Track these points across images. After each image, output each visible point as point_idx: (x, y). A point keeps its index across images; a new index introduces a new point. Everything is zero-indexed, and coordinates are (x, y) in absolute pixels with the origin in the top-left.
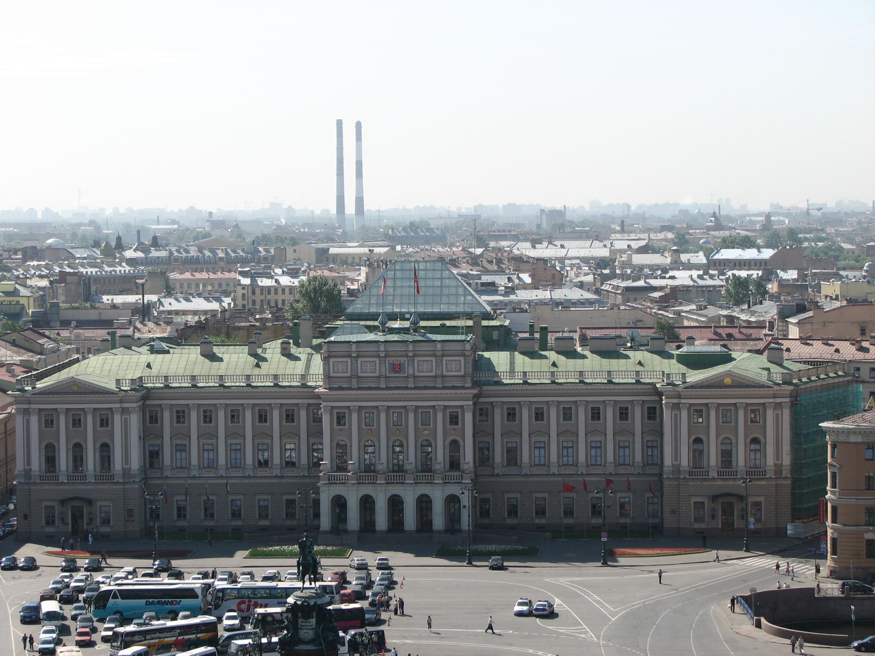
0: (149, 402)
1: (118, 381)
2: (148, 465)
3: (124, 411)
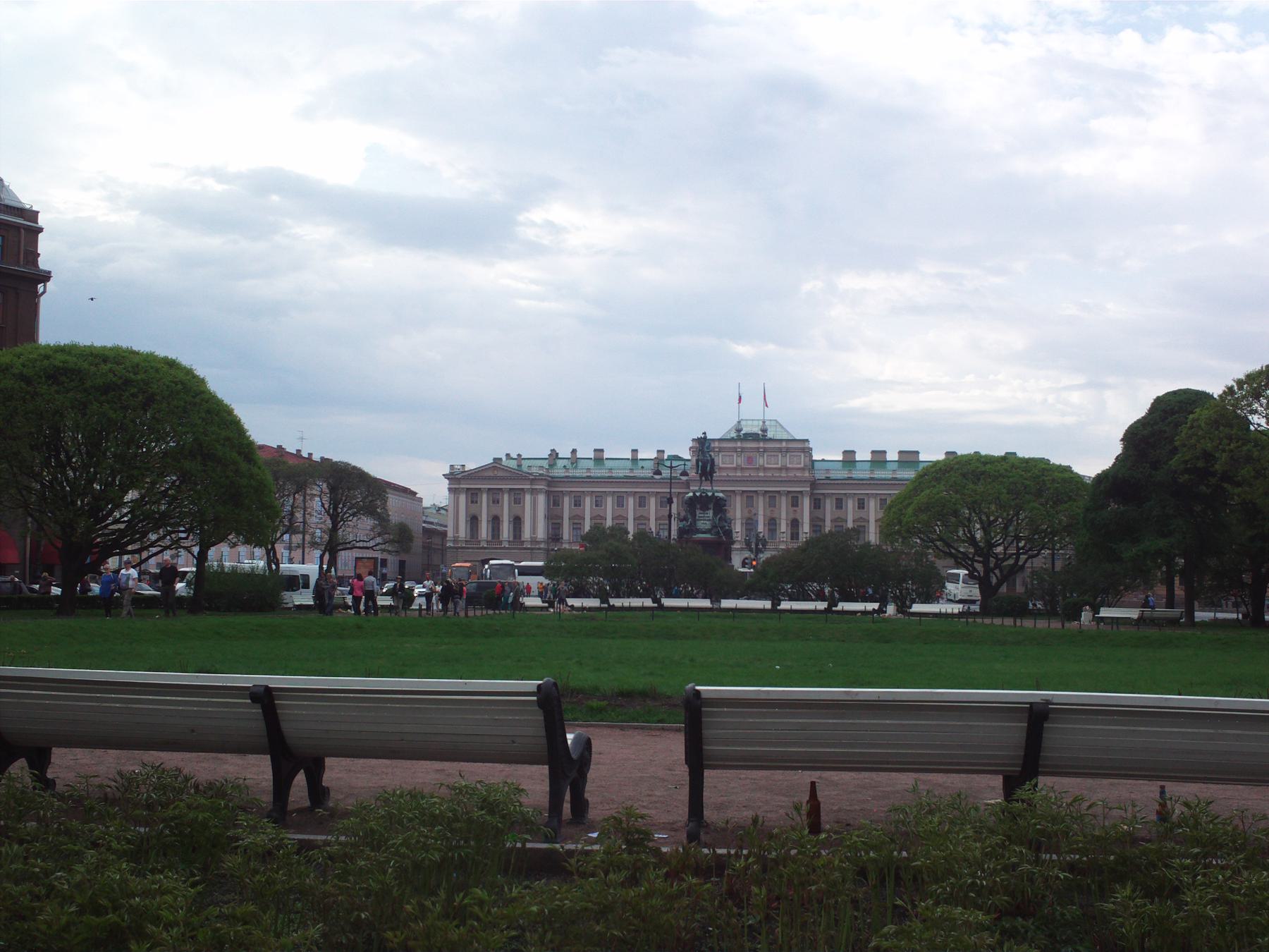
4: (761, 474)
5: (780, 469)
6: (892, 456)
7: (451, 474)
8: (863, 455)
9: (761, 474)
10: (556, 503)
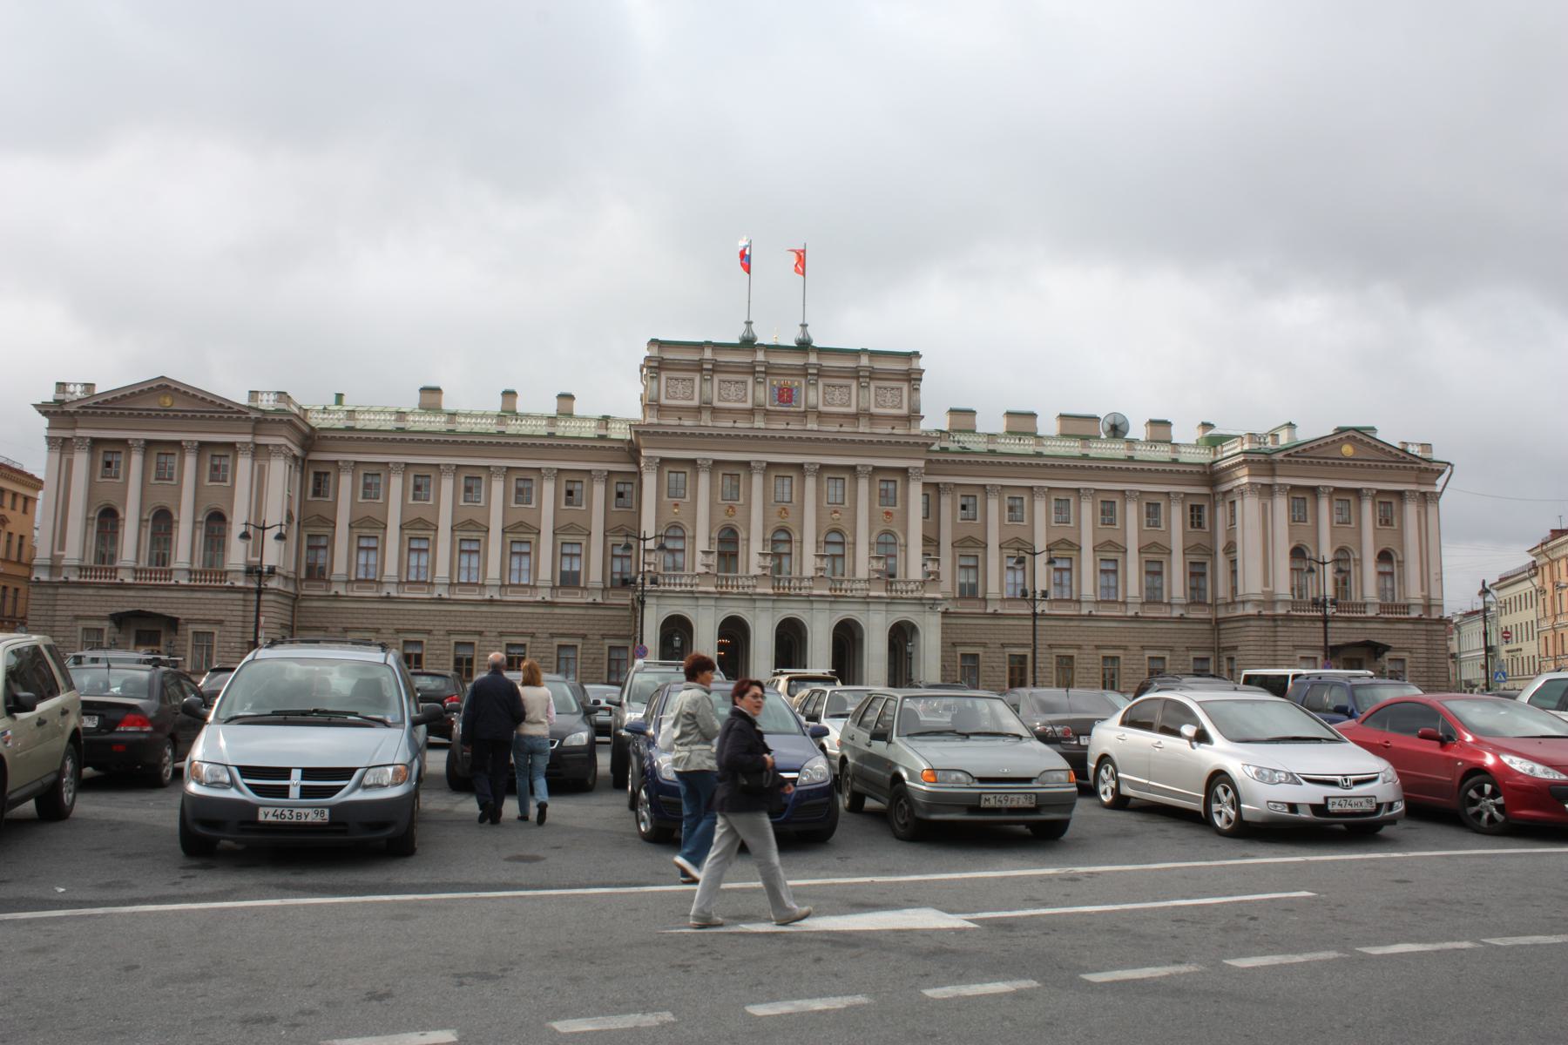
0: (314, 456)
1: (254, 394)
2: (303, 575)
3: (258, 451)
4: (812, 425)
5: (856, 417)
6: (1048, 425)
7: (60, 403)
8: (991, 421)
9: (812, 425)
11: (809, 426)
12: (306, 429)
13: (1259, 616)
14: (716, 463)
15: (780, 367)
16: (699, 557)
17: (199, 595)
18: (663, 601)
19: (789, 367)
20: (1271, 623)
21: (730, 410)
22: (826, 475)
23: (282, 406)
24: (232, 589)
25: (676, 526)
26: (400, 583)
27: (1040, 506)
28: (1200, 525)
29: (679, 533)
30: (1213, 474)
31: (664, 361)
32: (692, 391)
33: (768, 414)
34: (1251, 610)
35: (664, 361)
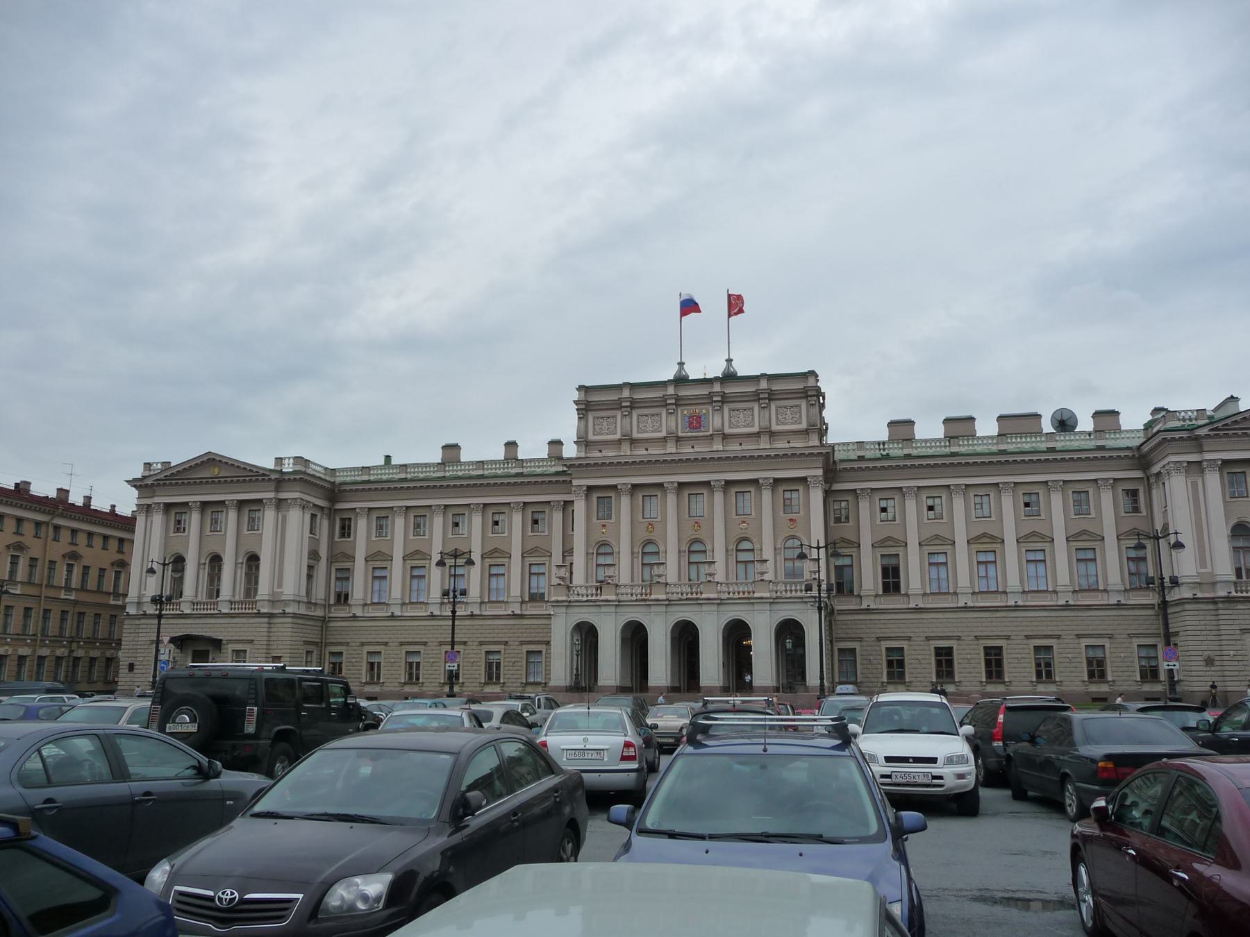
1: (279, 460)
2: (332, 602)
3: (280, 504)
10: (346, 530)
11: (715, 448)
12: (327, 485)
13: (1195, 600)
14: (635, 486)
15: (688, 398)
16: (554, 569)
17: (236, 620)
18: (571, 610)
19: (697, 397)
20: (1211, 607)
21: (646, 440)
22: (733, 490)
23: (298, 468)
24: (259, 615)
25: (649, 542)
26: (403, 604)
27: (1056, 500)
28: (1136, 509)
29: (609, 550)
30: (1143, 457)
31: (591, 402)
32: (613, 427)
33: (678, 439)
34: (1186, 593)
35: (591, 402)
